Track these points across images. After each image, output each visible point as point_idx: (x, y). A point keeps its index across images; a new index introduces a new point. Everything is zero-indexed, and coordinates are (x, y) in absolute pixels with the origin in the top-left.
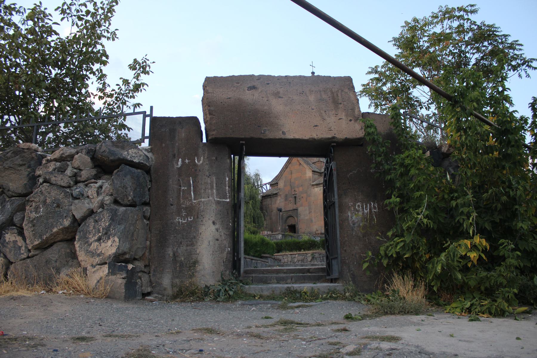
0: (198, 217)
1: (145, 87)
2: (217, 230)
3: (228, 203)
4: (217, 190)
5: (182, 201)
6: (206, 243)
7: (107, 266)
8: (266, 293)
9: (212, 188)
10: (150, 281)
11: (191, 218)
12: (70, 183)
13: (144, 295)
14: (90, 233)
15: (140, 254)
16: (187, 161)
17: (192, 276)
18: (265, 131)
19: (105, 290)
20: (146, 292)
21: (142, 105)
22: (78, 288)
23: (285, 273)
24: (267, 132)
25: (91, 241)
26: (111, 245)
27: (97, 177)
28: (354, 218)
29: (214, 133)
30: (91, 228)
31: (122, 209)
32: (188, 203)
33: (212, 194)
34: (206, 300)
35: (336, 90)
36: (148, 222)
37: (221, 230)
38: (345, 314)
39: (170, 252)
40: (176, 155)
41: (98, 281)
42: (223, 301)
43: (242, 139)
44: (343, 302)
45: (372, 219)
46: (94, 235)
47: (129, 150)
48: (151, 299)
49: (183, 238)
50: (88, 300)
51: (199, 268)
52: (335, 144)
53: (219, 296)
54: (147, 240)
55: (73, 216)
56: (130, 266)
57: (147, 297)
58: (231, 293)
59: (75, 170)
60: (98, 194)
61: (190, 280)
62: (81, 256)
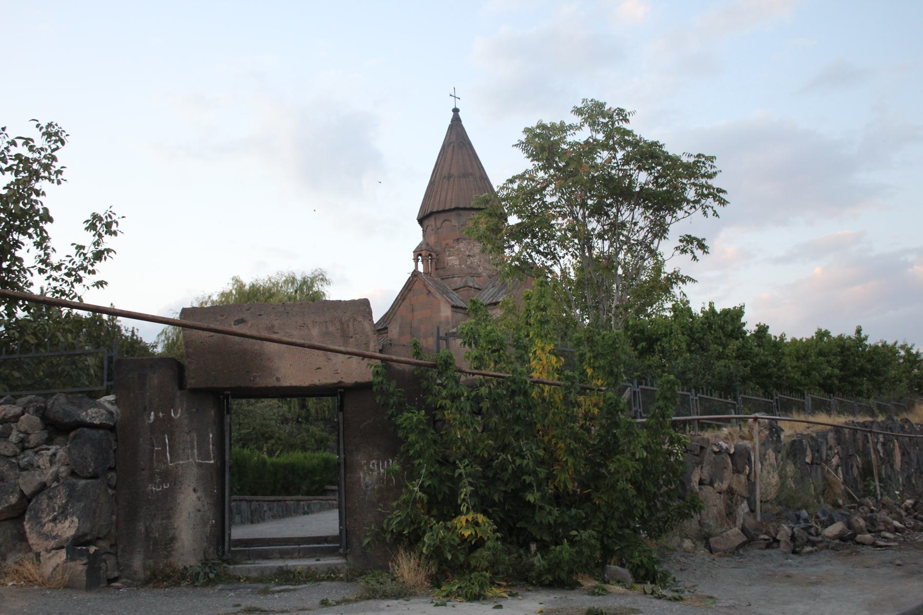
0: (175, 484)
1: (112, 254)
2: (199, 499)
3: (211, 465)
4: (198, 450)
5: (155, 464)
6: (185, 514)
7: (64, 550)
8: (254, 574)
9: (192, 448)
10: (118, 563)
11: (166, 485)
12: (16, 452)
13: (110, 581)
14: (43, 511)
15: (105, 532)
16: (161, 415)
17: (169, 555)
18: (255, 377)
19: (63, 578)
20: (112, 577)
21: (106, 283)
22: (31, 578)
23: (296, 543)
24: (257, 379)
25: (44, 521)
26: (69, 526)
27: (49, 441)
28: (367, 479)
29: (193, 381)
30: (44, 506)
31: (82, 482)
32: (163, 467)
33: (193, 455)
34: (183, 585)
35: (347, 319)
36: (114, 492)
37: (203, 498)
38: (322, 599)
39: (141, 527)
40: (148, 407)
41: (54, 569)
42: (202, 586)
43: (227, 389)
44: (339, 583)
45: (389, 480)
46: (48, 515)
47: (88, 409)
48: (118, 586)
49: (158, 510)
50: (43, 592)
51: (177, 545)
52: (342, 390)
53: (197, 579)
54: (112, 514)
55: (22, 491)
56: (92, 549)
57: (113, 584)
58: (212, 576)
59: (21, 435)
60: (52, 463)
61: (165, 561)
62: (33, 539)
